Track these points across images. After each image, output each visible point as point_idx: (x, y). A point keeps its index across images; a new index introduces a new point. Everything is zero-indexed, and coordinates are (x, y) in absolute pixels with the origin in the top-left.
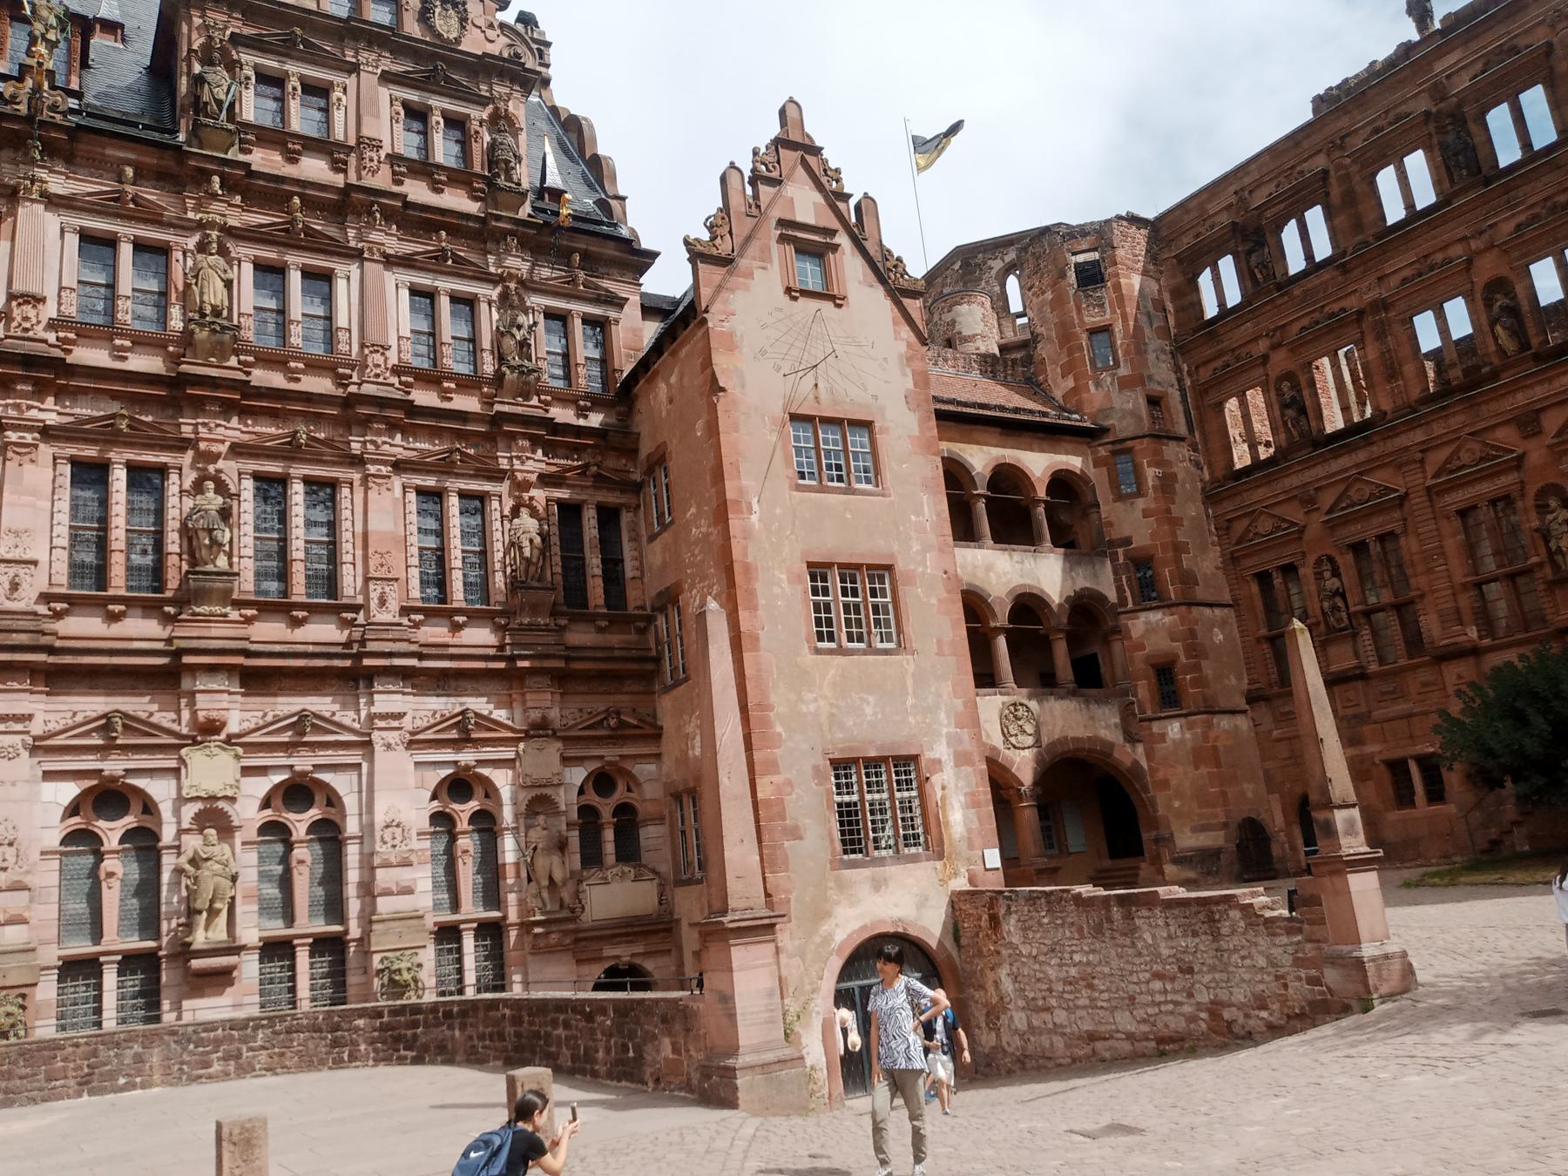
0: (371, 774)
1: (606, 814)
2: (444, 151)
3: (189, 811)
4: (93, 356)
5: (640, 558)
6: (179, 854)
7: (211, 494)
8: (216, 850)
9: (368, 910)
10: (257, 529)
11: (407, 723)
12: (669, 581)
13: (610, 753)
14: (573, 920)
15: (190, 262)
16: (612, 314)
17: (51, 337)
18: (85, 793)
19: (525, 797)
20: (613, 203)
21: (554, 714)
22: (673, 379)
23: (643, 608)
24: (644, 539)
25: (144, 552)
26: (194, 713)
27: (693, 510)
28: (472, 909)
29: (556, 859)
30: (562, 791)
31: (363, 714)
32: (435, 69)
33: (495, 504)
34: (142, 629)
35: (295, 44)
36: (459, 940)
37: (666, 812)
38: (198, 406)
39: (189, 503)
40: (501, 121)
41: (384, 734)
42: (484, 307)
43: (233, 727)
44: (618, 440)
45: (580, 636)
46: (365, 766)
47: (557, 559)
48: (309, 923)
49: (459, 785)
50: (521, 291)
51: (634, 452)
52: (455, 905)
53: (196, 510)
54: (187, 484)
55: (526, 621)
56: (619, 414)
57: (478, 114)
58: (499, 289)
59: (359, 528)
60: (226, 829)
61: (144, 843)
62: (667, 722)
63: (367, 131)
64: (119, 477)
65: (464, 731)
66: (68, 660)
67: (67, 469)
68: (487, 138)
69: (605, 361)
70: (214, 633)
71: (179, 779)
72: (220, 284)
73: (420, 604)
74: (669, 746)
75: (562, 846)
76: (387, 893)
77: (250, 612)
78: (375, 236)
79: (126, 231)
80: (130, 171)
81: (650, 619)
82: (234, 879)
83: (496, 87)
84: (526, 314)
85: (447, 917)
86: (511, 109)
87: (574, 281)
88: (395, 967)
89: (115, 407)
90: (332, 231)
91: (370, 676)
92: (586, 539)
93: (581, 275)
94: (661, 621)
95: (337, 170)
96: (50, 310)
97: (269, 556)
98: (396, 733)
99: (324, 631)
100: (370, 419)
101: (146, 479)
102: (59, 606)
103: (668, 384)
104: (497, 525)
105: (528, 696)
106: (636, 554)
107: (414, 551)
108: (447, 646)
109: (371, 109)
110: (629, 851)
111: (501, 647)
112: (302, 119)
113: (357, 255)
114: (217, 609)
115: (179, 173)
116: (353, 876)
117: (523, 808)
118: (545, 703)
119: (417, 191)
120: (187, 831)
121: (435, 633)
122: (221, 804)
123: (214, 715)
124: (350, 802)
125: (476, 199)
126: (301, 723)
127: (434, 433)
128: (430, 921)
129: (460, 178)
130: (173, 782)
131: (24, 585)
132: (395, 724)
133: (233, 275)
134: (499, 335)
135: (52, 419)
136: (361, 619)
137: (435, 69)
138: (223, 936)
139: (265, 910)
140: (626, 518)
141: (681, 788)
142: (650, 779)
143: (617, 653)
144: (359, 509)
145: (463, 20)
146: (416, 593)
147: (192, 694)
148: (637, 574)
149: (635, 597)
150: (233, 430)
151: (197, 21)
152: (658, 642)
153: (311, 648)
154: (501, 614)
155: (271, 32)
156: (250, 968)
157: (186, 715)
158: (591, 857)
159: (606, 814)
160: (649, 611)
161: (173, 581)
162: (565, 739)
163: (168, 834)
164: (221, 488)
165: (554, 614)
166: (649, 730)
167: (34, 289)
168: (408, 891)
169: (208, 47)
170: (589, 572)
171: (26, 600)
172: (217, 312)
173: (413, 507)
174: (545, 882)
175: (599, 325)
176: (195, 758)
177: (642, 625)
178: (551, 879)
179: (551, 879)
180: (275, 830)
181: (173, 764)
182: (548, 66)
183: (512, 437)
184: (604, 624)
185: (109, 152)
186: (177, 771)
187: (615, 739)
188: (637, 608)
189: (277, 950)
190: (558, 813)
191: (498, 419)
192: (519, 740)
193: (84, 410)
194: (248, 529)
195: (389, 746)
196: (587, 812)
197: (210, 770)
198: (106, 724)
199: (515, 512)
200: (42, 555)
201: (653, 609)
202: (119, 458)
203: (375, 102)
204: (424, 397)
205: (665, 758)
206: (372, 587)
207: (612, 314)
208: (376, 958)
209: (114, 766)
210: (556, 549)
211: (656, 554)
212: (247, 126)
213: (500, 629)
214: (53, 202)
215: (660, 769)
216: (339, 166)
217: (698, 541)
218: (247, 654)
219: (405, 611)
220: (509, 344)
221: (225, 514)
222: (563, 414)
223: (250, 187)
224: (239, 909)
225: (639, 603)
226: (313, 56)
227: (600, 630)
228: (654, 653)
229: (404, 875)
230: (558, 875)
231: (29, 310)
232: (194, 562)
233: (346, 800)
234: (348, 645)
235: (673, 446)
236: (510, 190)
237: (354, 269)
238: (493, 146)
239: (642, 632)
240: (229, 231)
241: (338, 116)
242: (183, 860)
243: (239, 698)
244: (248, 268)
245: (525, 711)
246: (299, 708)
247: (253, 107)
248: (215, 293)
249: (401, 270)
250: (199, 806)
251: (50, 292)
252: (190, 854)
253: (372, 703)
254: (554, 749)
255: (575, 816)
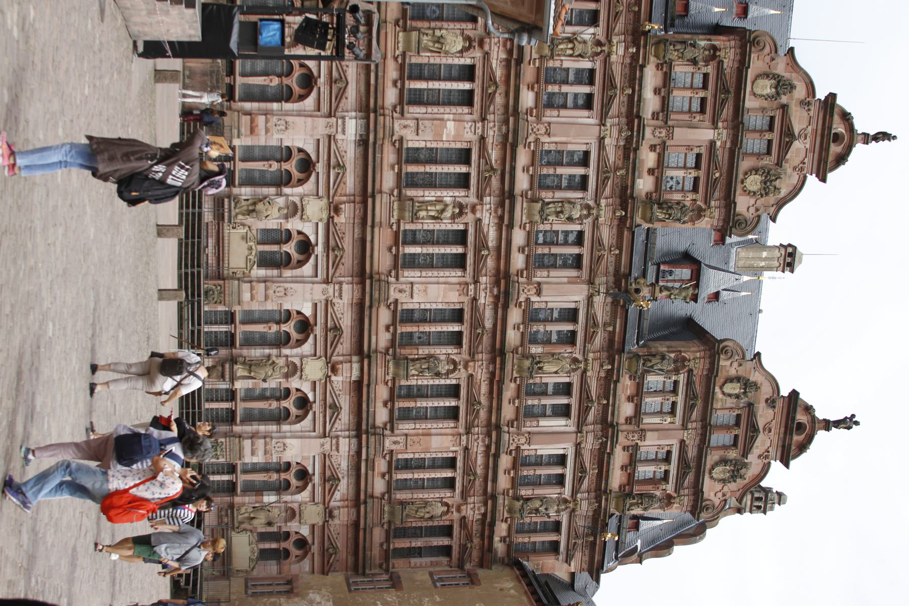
0: (310, 437)
1: (284, 545)
2: (645, 471)
3: (297, 361)
4: (515, 316)
5: (421, 567)
6: (277, 356)
7: (447, 368)
8: (277, 373)
9: (245, 435)
10: (432, 386)
11: (334, 453)
12: (404, 584)
13: (315, 549)
14: (233, 528)
15: (566, 355)
16: (561, 557)
17: (522, 299)
18: (307, 318)
19: (295, 506)
20: (635, 557)
21: (336, 521)
22: (512, 591)
23: (393, 567)
24: (432, 569)
25: (420, 338)
26: (342, 362)
27: (438, 599)
28: (242, 478)
29: (263, 521)
30: (297, 524)
31: (340, 433)
32: (692, 468)
33: (448, 495)
34: (383, 339)
35: (692, 399)
36: (228, 473)
37: (283, 575)
38: (493, 361)
39: (443, 357)
40: (668, 500)
41: (329, 443)
42: (558, 491)
43: (333, 378)
44: (487, 558)
45: (378, 535)
46: (313, 434)
47: (419, 524)
48: (241, 407)
49: (304, 475)
50: (568, 510)
51: (481, 565)
52: (245, 472)
53: (437, 359)
54: (452, 356)
55: (386, 508)
56: (503, 559)
57: (670, 488)
58: (569, 499)
59: (433, 431)
60: (287, 376)
61: (283, 341)
62: (330, 578)
63: (649, 434)
64: (455, 328)
65: (330, 480)
66: (367, 313)
67: (458, 307)
68: (658, 493)
69: (534, 550)
70: (379, 370)
71: (311, 356)
72: (555, 370)
73: (394, 459)
74: (318, 578)
75: (270, 524)
76: (253, 444)
77: (390, 384)
78: (590, 438)
79: (580, 328)
80: (611, 329)
81: (387, 571)
82: (264, 380)
83: (686, 498)
84: (556, 512)
85: (239, 468)
86: (675, 505)
87: (577, 537)
88: (219, 449)
89: (488, 324)
90: (591, 418)
91: (358, 437)
92: (432, 539)
93: (580, 542)
94: (385, 577)
95: (626, 419)
96: (534, 298)
97: (419, 390)
98: (329, 448)
99: (382, 415)
100: (490, 436)
101: (456, 339)
102: (392, 307)
103: (511, 588)
104: (437, 495)
105: (346, 509)
106: (424, 564)
107: (422, 456)
108: (373, 470)
109: (662, 436)
110: (265, 555)
111: (372, 497)
112: (651, 402)
113: (579, 431)
114: (391, 370)
115: (614, 349)
116: (262, 428)
117: (289, 505)
118: (343, 517)
119: (620, 457)
120: (287, 360)
121: (381, 465)
122: (299, 373)
123: (340, 372)
124: (297, 427)
125: (620, 487)
126: (335, 408)
127: (486, 466)
128: (239, 462)
129: (631, 479)
130: (309, 353)
131: (401, 294)
132: (334, 448)
133: (561, 374)
134: (542, 499)
135: (482, 301)
136: (387, 432)
137: (692, 468)
138: (238, 375)
139: (248, 390)
140: (444, 560)
141: (294, 584)
142: (302, 568)
143: (368, 553)
144: (443, 431)
145: (723, 481)
146: (400, 456)
147: (351, 362)
148: (413, 565)
149: (399, 565)
150: (481, 374)
151: (698, 355)
152: (374, 575)
153: (371, 410)
154: (390, 497)
155: (699, 388)
156: (223, 386)
157: (341, 358)
158: (263, 537)
159: (284, 545)
160: (391, 570)
161: (406, 351)
162: (323, 526)
163: (286, 351)
164: (449, 372)
165: (389, 522)
166: (326, 570)
167: (544, 292)
168: (253, 453)
169: (684, 359)
170: (413, 540)
171: (393, 295)
172: (540, 368)
173: (445, 455)
174: (252, 515)
175: (554, 547)
176: (321, 363)
177: (384, 566)
178: (253, 518)
179: (253, 518)
180: (287, 393)
181: (318, 354)
182: (751, 512)
183: (486, 504)
184: (385, 547)
185: (618, 321)
186: (315, 355)
187: (323, 551)
188: (393, 565)
189: (231, 395)
190: (286, 522)
191: (494, 497)
192: (324, 504)
193: (488, 313)
194: (431, 382)
195: (322, 445)
196: (287, 535)
197: (315, 369)
198: (337, 329)
199: (447, 504)
200: (416, 298)
201: (392, 573)
202: (464, 328)
203: (666, 438)
204: (505, 461)
205: (311, 576)
206: (403, 437)
207: (562, 557)
208: (223, 440)
209: (318, 330)
210: (425, 524)
211: (422, 576)
212: (642, 378)
213: (383, 495)
214: (590, 298)
215: (306, 573)
216: (629, 420)
217: (421, 601)
218: (369, 385)
219: (392, 451)
220: (537, 504)
221: (438, 375)
222: (501, 529)
223: (609, 382)
224: (251, 381)
225: (396, 565)
226: (689, 408)
227: (381, 545)
228: (367, 571)
229: (261, 452)
230: (255, 522)
231: (534, 290)
232: (413, 360)
233: (298, 425)
234: (374, 427)
235: (477, 590)
236: (624, 506)
237: (573, 429)
238: (651, 497)
239: (381, 566)
240: (585, 371)
241: (657, 420)
242: (274, 358)
243: (348, 380)
244: (567, 380)
245: (339, 508)
246: (343, 406)
247: (654, 380)
248: (547, 368)
249: (574, 451)
250: (299, 365)
251: (543, 299)
252: (277, 361)
253: (344, 437)
254: (318, 520)
255: (284, 529)
